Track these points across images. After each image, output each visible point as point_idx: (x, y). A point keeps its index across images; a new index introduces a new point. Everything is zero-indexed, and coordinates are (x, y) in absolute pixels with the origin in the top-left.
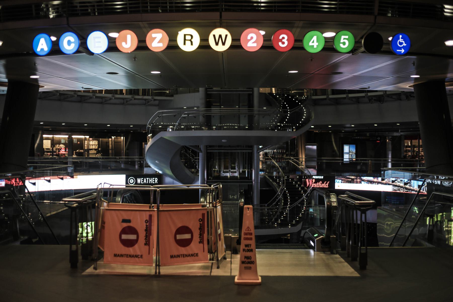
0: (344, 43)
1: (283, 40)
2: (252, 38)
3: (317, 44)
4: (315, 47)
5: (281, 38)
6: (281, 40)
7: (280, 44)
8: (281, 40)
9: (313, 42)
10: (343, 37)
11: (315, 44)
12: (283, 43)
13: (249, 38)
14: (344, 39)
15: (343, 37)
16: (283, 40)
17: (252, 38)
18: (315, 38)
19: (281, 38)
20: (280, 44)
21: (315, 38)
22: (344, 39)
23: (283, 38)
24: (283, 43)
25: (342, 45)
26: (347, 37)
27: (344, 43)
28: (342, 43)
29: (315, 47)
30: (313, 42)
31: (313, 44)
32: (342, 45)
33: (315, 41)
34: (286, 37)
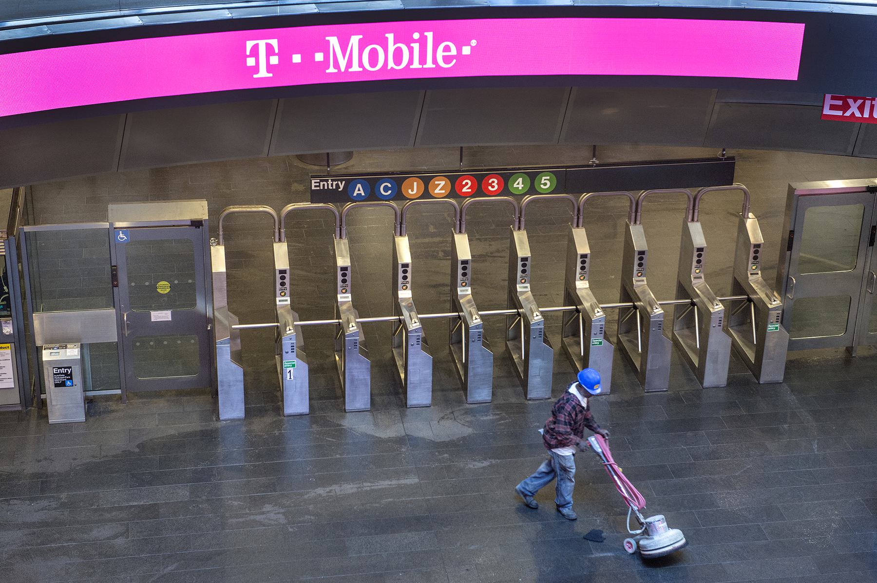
0: (545, 184)
1: (493, 184)
2: (467, 184)
3: (523, 186)
4: (520, 188)
5: (490, 181)
6: (490, 185)
7: (490, 188)
8: (490, 185)
9: (518, 184)
10: (544, 178)
11: (521, 186)
12: (493, 187)
13: (464, 183)
14: (545, 180)
15: (544, 178)
16: (493, 184)
17: (467, 184)
18: (520, 180)
19: (490, 181)
20: (490, 188)
21: (520, 180)
22: (545, 180)
23: (493, 182)
24: (493, 187)
25: (542, 186)
26: (548, 178)
27: (545, 184)
28: (542, 184)
29: (520, 188)
30: (518, 184)
31: (518, 186)
32: (542, 186)
33: (521, 183)
34: (496, 181)
